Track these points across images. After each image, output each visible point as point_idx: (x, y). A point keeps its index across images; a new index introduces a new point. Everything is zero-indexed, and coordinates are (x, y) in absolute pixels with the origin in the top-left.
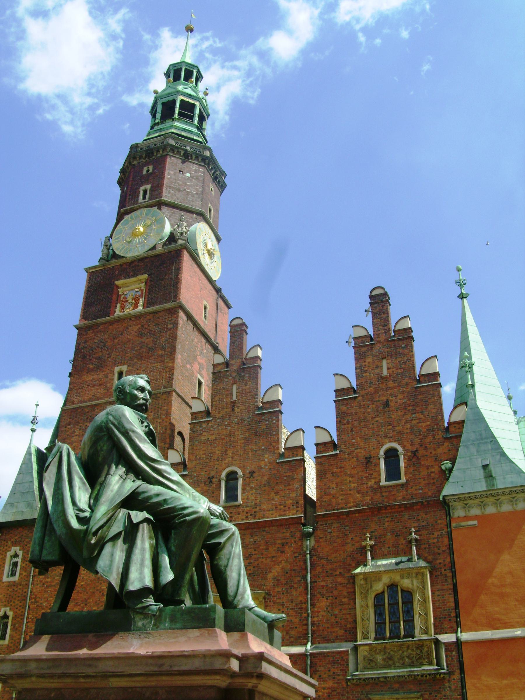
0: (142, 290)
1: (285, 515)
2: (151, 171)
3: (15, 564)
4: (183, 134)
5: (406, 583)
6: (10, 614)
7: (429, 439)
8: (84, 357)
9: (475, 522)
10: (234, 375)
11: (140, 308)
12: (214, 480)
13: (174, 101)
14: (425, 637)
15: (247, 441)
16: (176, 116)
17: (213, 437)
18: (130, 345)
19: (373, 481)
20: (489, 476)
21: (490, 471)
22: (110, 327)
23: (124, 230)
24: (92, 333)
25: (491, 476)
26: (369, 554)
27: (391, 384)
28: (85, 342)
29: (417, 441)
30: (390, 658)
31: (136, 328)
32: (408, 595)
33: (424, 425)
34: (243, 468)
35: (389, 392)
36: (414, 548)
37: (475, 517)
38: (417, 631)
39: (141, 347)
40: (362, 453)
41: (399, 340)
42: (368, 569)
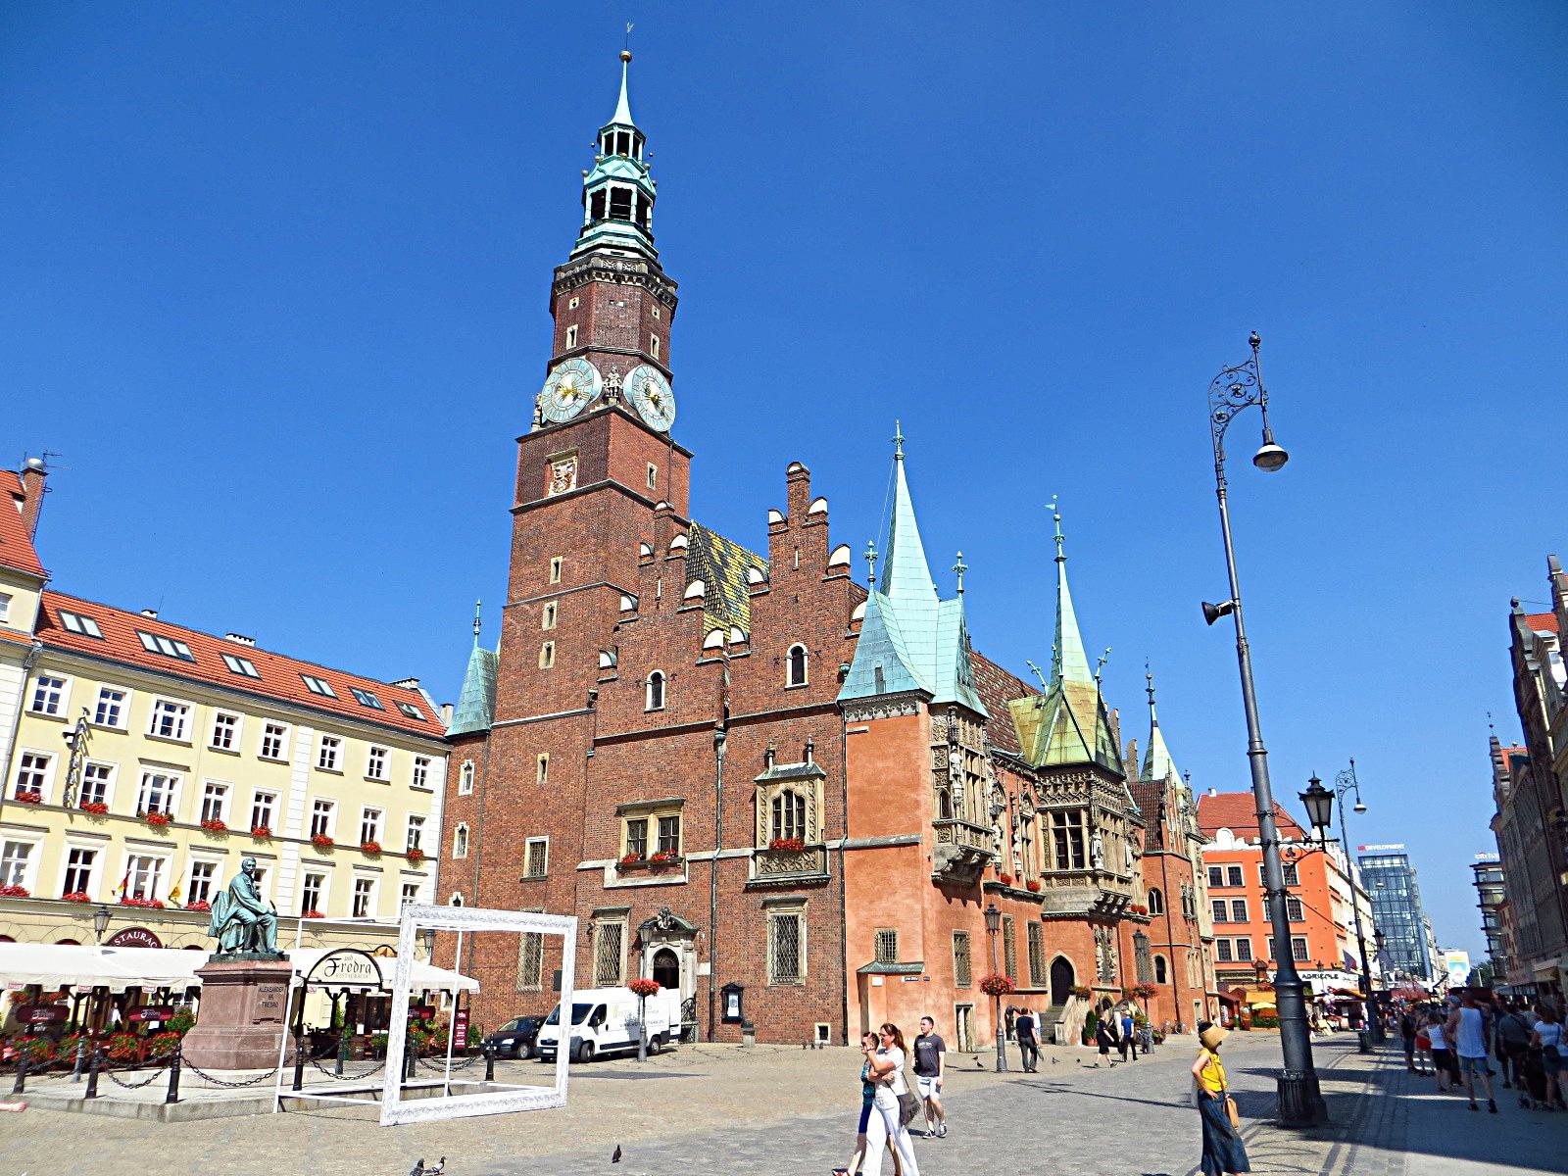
1: (702, 720)
3: (469, 776)
4: (616, 241)
6: (467, 828)
8: (521, 546)
10: (659, 567)
13: (604, 191)
14: (812, 843)
15: (670, 639)
16: (607, 216)
20: (880, 681)
27: (802, 577)
34: (665, 670)
38: (807, 837)
40: (771, 652)
42: (768, 777)
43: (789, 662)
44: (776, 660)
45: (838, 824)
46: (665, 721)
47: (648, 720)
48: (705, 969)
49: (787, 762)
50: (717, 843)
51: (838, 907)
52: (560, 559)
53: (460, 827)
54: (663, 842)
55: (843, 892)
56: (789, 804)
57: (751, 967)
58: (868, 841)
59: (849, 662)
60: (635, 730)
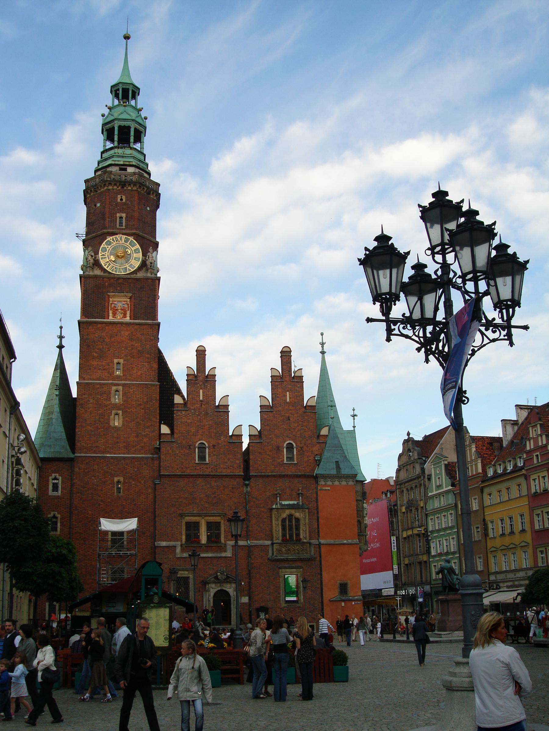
0: (128, 304)
2: (124, 201)
5: (297, 515)
6: (59, 516)
7: (309, 442)
8: (88, 346)
9: (329, 488)
11: (128, 318)
12: (191, 447)
13: (129, 128)
14: (305, 540)
18: (124, 345)
19: (280, 460)
20: (338, 467)
21: (339, 465)
22: (107, 327)
23: (108, 249)
24: (93, 329)
25: (339, 467)
26: (278, 498)
27: (291, 408)
28: (87, 335)
31: (127, 333)
32: (297, 520)
35: (290, 412)
36: (300, 498)
37: (329, 486)
38: (301, 537)
39: (132, 348)
43: (285, 450)
44: (279, 449)
45: (316, 532)
48: (245, 600)
49: (285, 500)
51: (319, 571)
52: (121, 361)
55: (321, 564)
56: (290, 521)
57: (272, 599)
58: (332, 541)
59: (321, 455)
60: (188, 472)
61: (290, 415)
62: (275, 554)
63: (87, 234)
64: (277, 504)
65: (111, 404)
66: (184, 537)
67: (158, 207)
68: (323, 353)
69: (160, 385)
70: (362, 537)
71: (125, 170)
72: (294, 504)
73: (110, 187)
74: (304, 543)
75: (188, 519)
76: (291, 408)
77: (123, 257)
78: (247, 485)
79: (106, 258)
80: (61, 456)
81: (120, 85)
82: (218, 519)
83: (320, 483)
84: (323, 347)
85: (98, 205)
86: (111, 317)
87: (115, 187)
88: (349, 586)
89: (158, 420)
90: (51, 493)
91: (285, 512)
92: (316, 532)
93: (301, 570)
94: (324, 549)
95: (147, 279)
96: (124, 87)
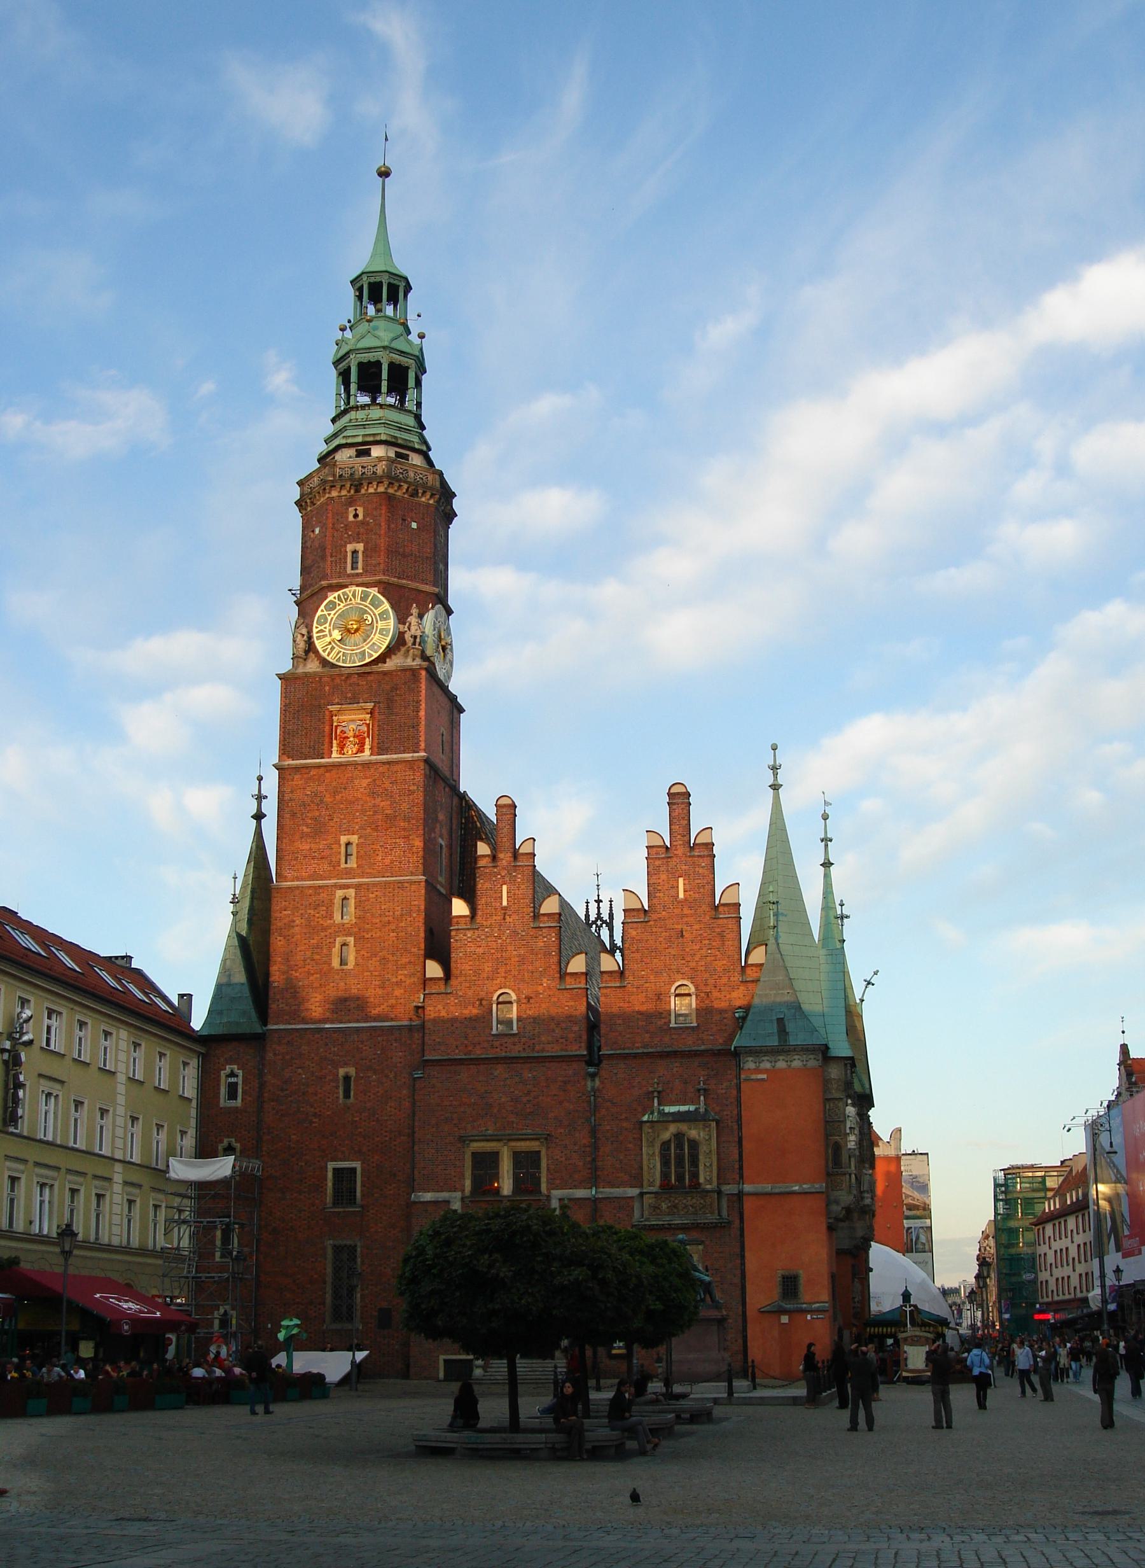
5: (693, 1133)
7: (724, 980)
8: (294, 815)
9: (765, 1076)
11: (367, 752)
12: (484, 1003)
13: (378, 364)
14: (708, 1187)
15: (522, 960)
17: (481, 950)
20: (782, 1031)
22: (327, 775)
26: (656, 1101)
27: (686, 911)
28: (292, 792)
29: (711, 981)
30: (675, 1206)
31: (365, 782)
32: (694, 1145)
33: (720, 963)
34: (518, 992)
36: (702, 1098)
37: (766, 1071)
38: (702, 1180)
39: (375, 812)
41: (699, 856)
46: (519, 1047)
47: (496, 1044)
50: (593, 1180)
51: (738, 1250)
53: (226, 1141)
54: (516, 1180)
55: (742, 1235)
56: (680, 1146)
58: (768, 1188)
60: (478, 1053)
61: (685, 927)
62: (646, 1213)
63: (303, 588)
64: (652, 1113)
65: (334, 925)
66: (468, 1183)
67: (450, 516)
68: (775, 787)
69: (426, 881)
70: (843, 1178)
71: (367, 453)
72: (689, 1112)
73: (334, 494)
74: (708, 1192)
75: (476, 1146)
76: (686, 911)
77: (357, 630)
78: (593, 1076)
79: (325, 636)
80: (240, 1031)
81: (365, 278)
82: (533, 1145)
83: (747, 1066)
84: (776, 775)
85: (317, 531)
86: (334, 755)
87: (344, 493)
88: (802, 1281)
89: (422, 952)
90: (224, 1101)
91: (667, 1129)
92: (733, 1167)
93: (701, 1247)
94: (748, 1205)
95: (405, 670)
96: (372, 280)
